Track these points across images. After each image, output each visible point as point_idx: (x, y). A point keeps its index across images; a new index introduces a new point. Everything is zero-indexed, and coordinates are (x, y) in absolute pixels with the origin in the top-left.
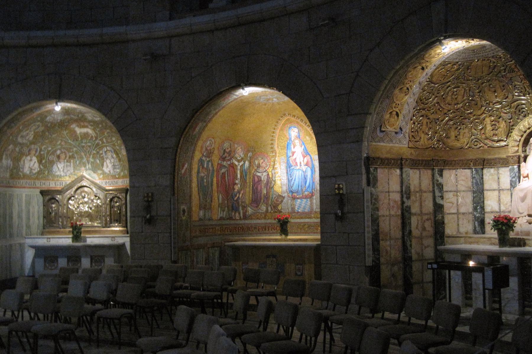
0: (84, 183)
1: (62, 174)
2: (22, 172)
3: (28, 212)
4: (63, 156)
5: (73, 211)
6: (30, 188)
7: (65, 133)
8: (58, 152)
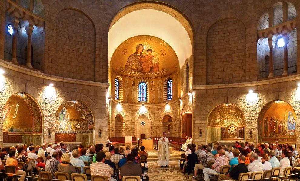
0: (232, 126)
1: (226, 123)
3: (218, 133)
4: (226, 118)
7: (227, 112)
8: (225, 117)
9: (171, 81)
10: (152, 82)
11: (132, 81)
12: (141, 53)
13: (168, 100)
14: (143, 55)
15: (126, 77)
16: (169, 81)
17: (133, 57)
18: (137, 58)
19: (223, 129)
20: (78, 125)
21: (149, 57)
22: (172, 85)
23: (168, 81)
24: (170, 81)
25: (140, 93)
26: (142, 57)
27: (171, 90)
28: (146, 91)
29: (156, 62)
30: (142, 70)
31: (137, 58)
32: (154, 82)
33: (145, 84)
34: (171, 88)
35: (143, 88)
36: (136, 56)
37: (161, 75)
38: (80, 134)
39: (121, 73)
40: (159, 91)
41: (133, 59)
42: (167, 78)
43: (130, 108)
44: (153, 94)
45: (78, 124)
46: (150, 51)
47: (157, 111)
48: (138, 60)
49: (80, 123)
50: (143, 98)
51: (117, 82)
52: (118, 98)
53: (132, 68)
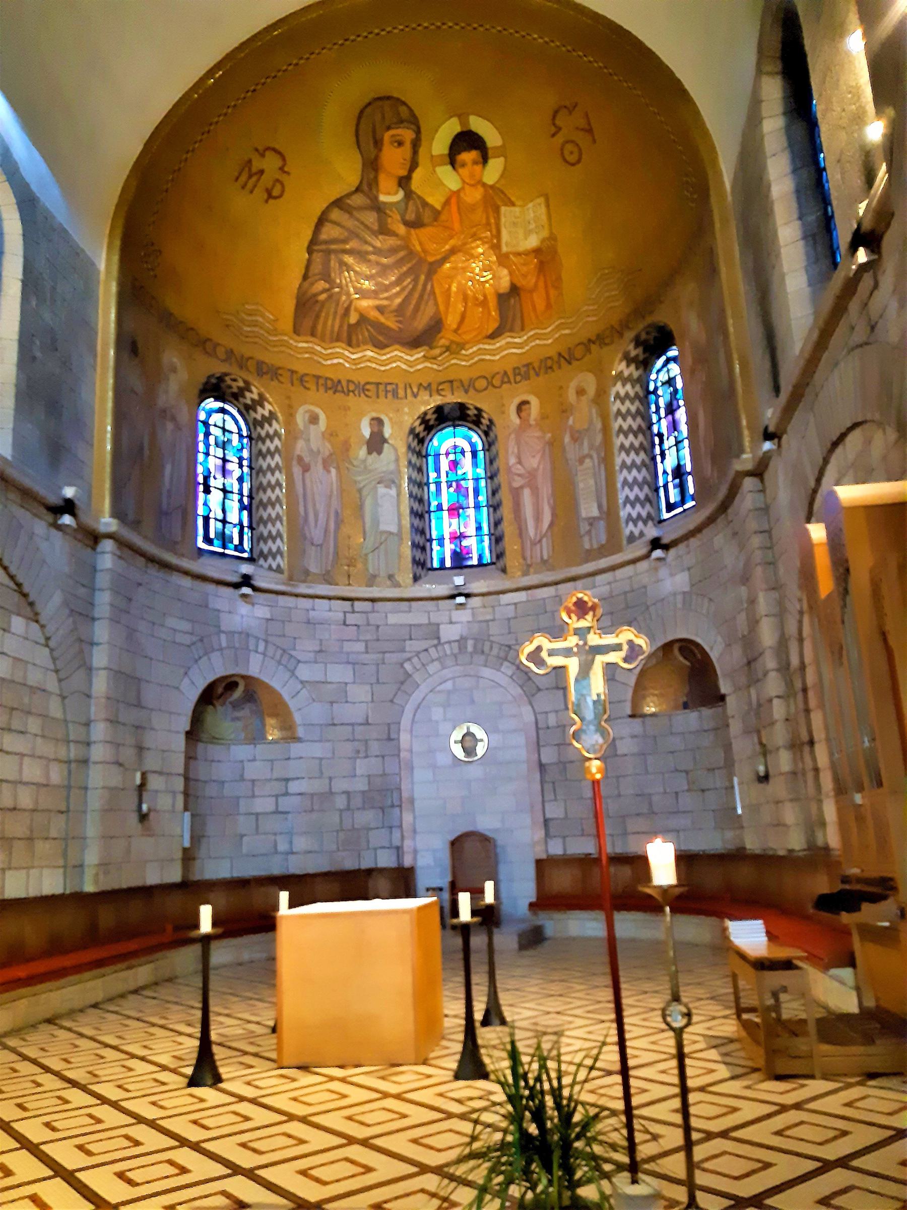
9: (674, 359)
10: (522, 406)
11: (362, 415)
12: (404, 182)
13: (666, 515)
14: (425, 204)
18: (384, 230)
21: (472, 208)
22: (679, 384)
23: (646, 365)
25: (440, 508)
27: (684, 428)
28: (482, 483)
29: (533, 242)
30: (436, 326)
32: (534, 402)
33: (475, 438)
34: (681, 415)
35: (454, 465)
36: (371, 218)
37: (590, 332)
39: (260, 356)
40: (581, 461)
42: (638, 342)
43: (351, 619)
48: (393, 251)
50: (465, 543)
51: (231, 425)
53: (353, 318)
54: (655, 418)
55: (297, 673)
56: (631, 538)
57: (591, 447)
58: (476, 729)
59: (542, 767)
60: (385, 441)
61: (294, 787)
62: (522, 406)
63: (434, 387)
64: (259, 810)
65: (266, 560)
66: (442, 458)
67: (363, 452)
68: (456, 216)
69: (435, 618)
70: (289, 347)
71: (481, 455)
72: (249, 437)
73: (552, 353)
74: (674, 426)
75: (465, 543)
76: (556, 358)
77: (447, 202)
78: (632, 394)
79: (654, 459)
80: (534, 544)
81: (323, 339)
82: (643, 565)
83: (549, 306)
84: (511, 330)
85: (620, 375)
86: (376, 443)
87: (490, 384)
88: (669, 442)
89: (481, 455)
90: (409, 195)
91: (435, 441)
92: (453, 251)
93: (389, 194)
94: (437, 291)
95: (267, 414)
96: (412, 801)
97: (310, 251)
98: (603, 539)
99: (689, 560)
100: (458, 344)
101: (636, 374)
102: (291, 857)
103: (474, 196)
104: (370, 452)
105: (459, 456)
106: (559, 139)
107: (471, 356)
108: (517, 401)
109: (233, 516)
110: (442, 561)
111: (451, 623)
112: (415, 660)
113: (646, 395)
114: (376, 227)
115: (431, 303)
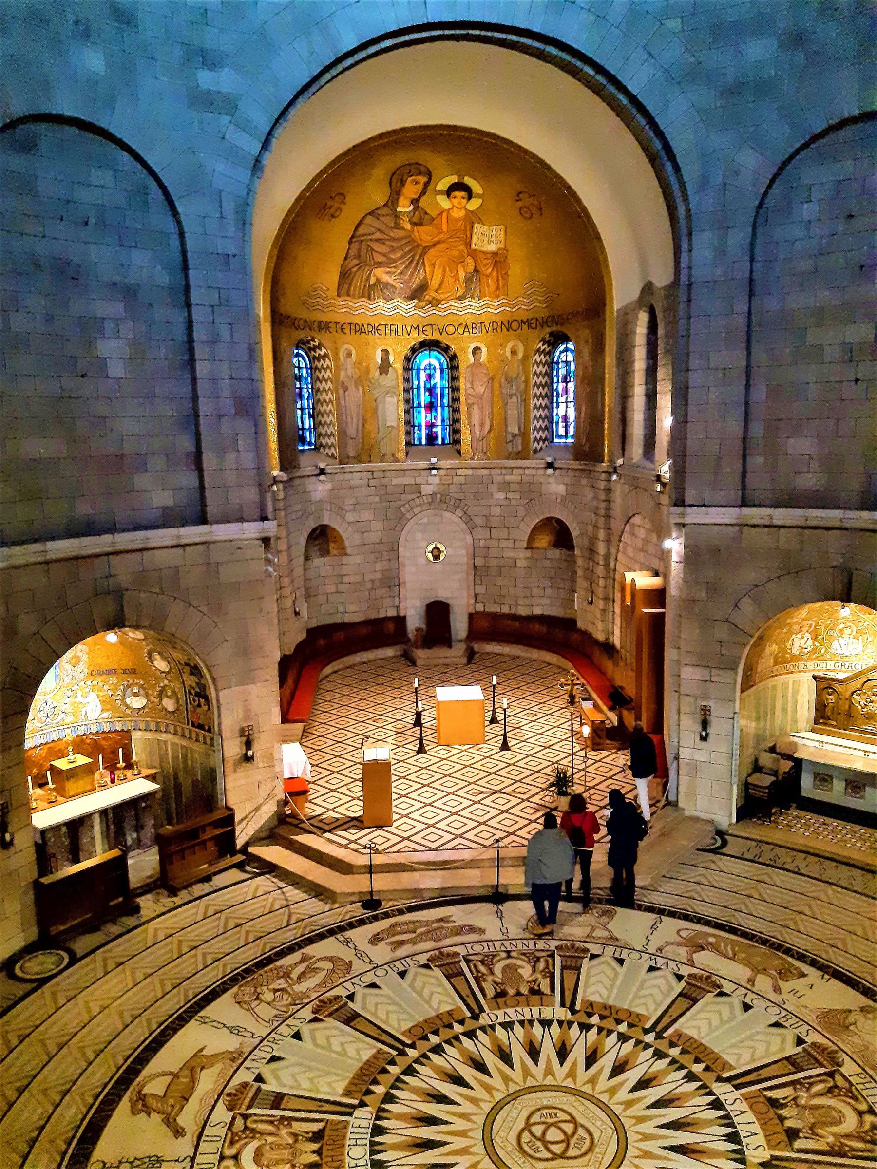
2: (790, 654)
5: (858, 711)
6: (799, 672)
10: (476, 350)
11: (375, 348)
13: (556, 440)
15: (347, 331)
16: (562, 347)
17: (376, 223)
19: (824, 684)
20: (136, 695)
21: (457, 220)
22: (572, 367)
23: (554, 345)
24: (566, 350)
25: (419, 405)
26: (420, 224)
28: (446, 391)
29: (492, 248)
31: (397, 226)
32: (484, 350)
33: (443, 360)
38: (149, 736)
40: (511, 396)
41: (378, 235)
43: (372, 483)
44: (481, 409)
45: (135, 690)
46: (463, 194)
47: (502, 496)
49: (141, 686)
50: (434, 430)
51: (303, 365)
52: (310, 444)
53: (372, 281)
54: (555, 380)
55: (346, 518)
56: (536, 451)
57: (517, 390)
58: (439, 546)
59: (475, 567)
60: (390, 365)
61: (346, 579)
62: (476, 350)
63: (420, 327)
64: (328, 591)
65: (324, 448)
66: (422, 372)
67: (378, 372)
68: (444, 220)
69: (418, 480)
70: (334, 306)
71: (446, 371)
72: (311, 368)
73: (498, 319)
74: (566, 391)
75: (434, 430)
76: (499, 324)
77: (441, 214)
78: (544, 361)
79: (552, 403)
80: (479, 441)
81: (354, 297)
82: (541, 472)
83: (498, 288)
84: (472, 297)
85: (538, 350)
86: (385, 367)
87: (456, 330)
88: (562, 399)
89: (446, 371)
90: (416, 208)
91: (417, 360)
92: (439, 242)
93: (404, 207)
94: (427, 264)
95: (322, 353)
96: (404, 583)
97: (350, 242)
98: (520, 448)
99: (567, 480)
100: (437, 300)
101: (547, 350)
102: (346, 615)
103: (458, 214)
104: (381, 374)
105: (432, 371)
106: (520, 204)
107: (446, 309)
108: (473, 346)
109: (307, 426)
110: (420, 440)
111: (427, 484)
112: (407, 505)
113: (551, 364)
114: (392, 225)
115: (422, 271)
